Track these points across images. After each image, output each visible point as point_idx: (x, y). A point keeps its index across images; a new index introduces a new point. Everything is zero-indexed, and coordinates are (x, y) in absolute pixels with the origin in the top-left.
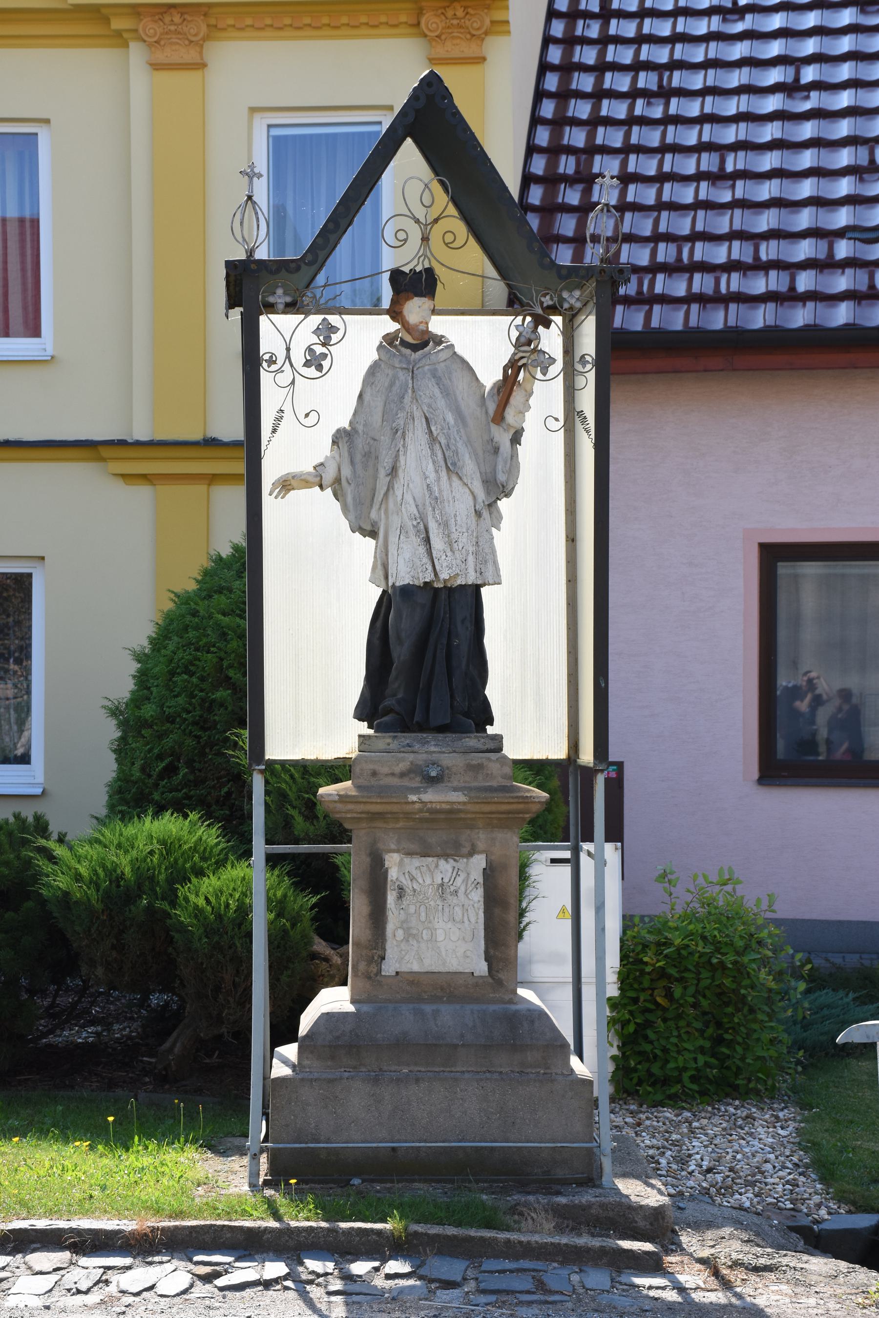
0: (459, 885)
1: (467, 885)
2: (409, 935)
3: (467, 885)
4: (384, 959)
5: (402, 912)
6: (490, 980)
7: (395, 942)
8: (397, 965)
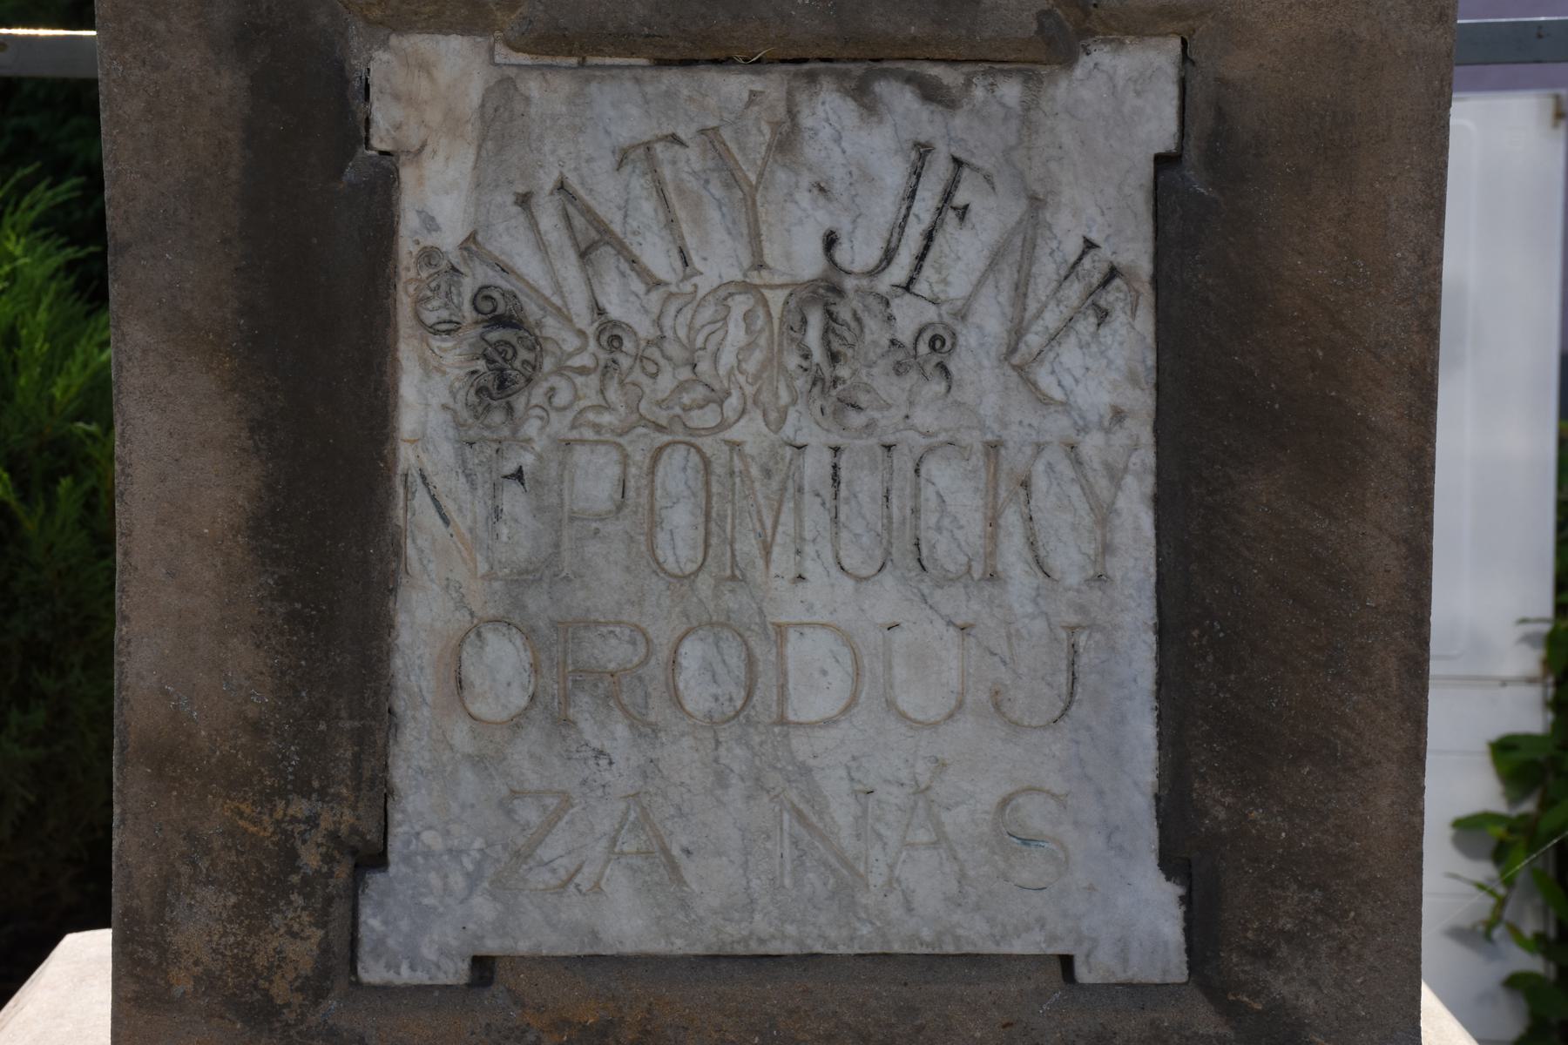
0: (958, 288)
1: (1021, 291)
2: (571, 680)
3: (1021, 291)
4: (379, 860)
5: (514, 499)
6: (1205, 1019)
7: (461, 735)
8: (484, 908)
